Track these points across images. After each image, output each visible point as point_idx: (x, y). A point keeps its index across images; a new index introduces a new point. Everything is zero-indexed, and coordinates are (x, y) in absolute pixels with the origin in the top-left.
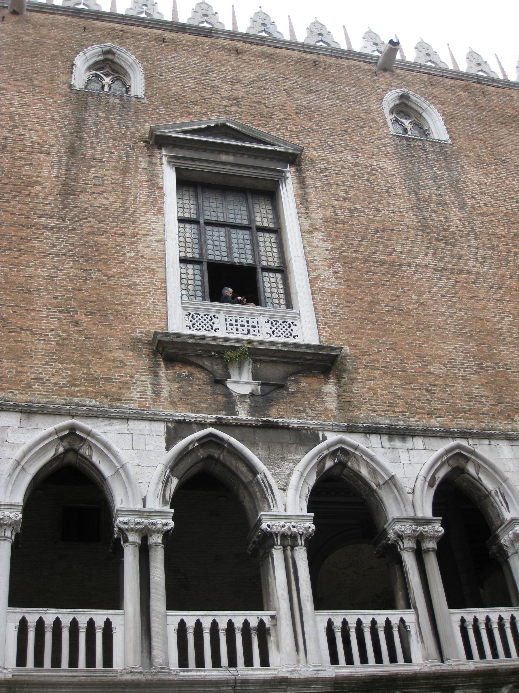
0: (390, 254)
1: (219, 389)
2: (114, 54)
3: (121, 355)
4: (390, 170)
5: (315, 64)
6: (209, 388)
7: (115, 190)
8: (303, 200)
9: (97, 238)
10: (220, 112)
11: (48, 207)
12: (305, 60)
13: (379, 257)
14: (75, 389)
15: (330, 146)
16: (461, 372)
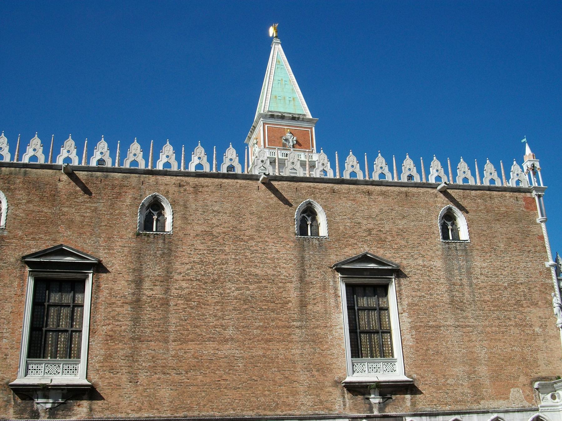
0: (435, 321)
1: (367, 401)
2: (312, 204)
3: (331, 389)
4: (439, 267)
5: (407, 194)
6: (363, 401)
7: (321, 301)
8: (399, 294)
9: (317, 330)
10: (362, 241)
11: (296, 316)
12: (402, 192)
13: (431, 323)
14: (316, 407)
15: (412, 256)
16: (461, 382)
